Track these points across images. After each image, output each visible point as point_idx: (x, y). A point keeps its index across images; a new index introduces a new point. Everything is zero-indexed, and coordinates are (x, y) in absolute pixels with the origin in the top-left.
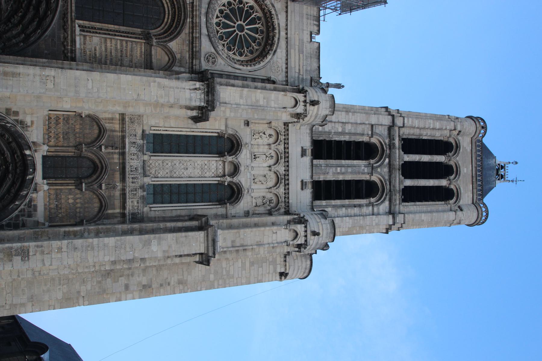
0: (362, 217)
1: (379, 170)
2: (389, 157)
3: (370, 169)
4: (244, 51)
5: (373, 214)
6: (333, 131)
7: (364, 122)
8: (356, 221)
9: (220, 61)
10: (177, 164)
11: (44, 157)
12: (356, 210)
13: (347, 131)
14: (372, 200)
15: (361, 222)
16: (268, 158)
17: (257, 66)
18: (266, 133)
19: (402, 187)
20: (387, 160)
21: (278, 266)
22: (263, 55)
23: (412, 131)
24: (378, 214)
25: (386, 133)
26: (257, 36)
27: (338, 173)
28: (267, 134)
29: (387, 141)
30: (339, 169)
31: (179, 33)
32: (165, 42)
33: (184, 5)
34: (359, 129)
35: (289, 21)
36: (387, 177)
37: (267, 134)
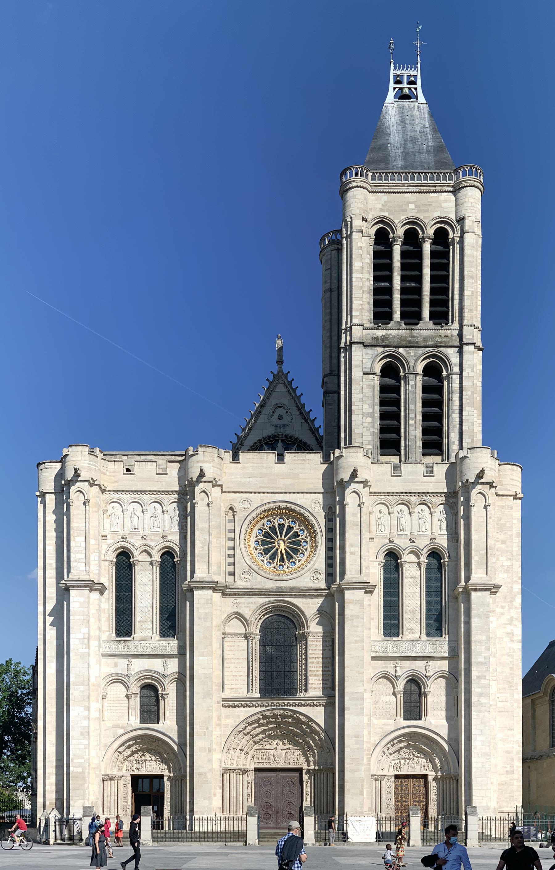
0: (464, 393)
1: (412, 364)
2: (398, 347)
3: (411, 377)
4: (303, 539)
5: (461, 373)
6: (372, 430)
7: (360, 388)
8: (468, 401)
9: (316, 567)
10: (409, 609)
11: (404, 719)
12: (456, 398)
13: (371, 411)
14: (444, 373)
15: (469, 393)
16: (403, 516)
17: (317, 527)
18: (379, 517)
19: (431, 325)
20: (401, 350)
21: (507, 503)
22: (305, 521)
23: (366, 306)
24: (461, 365)
25: (370, 351)
26: (286, 525)
27: (415, 422)
28: (380, 516)
29: (380, 350)
30: (411, 422)
31: (298, 608)
32: (307, 622)
33: (271, 603)
34: (368, 392)
35: (269, 491)
36: (421, 351)
37: (380, 516)
